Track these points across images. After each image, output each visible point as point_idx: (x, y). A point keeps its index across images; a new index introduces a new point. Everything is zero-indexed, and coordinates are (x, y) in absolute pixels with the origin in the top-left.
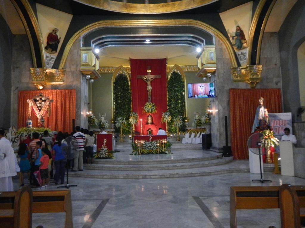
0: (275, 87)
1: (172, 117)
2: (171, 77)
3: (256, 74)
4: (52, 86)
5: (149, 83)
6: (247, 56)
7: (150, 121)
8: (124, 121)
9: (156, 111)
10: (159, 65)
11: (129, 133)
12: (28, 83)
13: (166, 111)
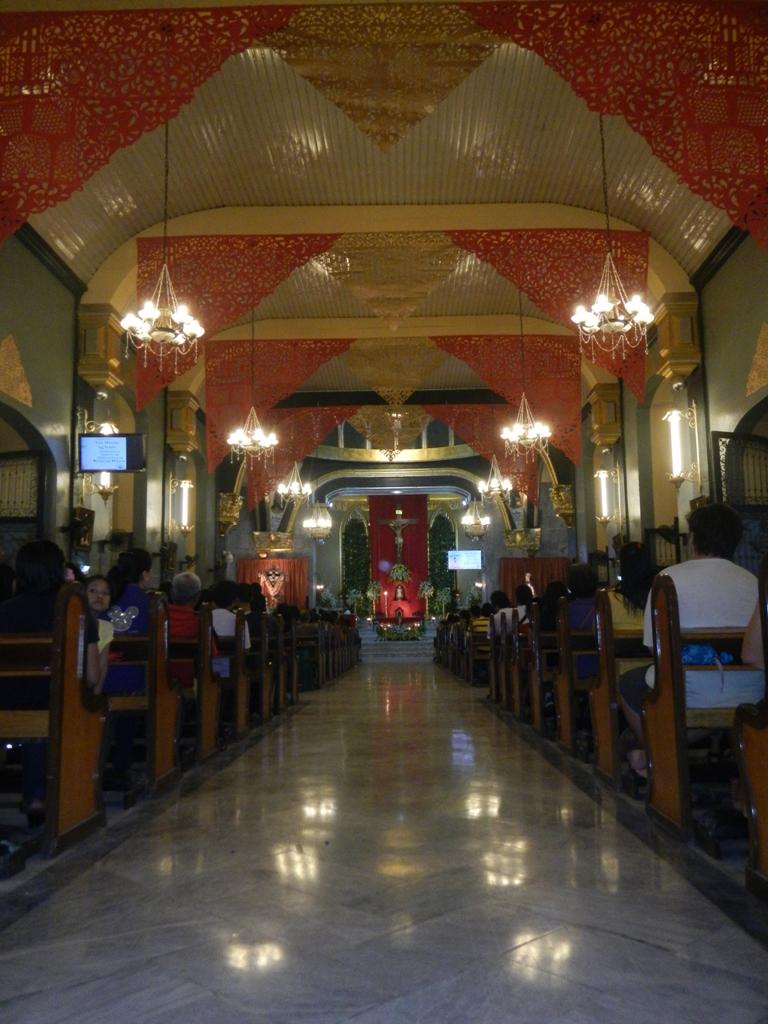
0: (561, 555)
1: (436, 589)
3: (533, 540)
4: (277, 553)
5: (399, 532)
6: (522, 518)
7: (400, 595)
8: (360, 595)
9: (410, 579)
10: (416, 505)
11: (368, 615)
12: (247, 549)
13: (424, 578)
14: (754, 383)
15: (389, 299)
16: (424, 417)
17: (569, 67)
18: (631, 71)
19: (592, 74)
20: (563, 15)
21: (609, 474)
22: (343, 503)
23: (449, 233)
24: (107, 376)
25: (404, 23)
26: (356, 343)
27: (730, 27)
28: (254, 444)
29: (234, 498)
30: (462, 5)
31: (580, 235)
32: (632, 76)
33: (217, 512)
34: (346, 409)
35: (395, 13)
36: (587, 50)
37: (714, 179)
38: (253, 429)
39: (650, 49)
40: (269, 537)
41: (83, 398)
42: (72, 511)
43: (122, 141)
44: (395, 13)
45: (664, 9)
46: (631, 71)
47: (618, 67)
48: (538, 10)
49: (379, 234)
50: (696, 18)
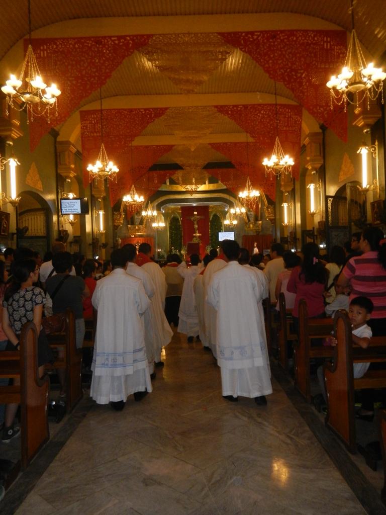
2: (213, 218)
5: (195, 222)
10: (203, 210)
14: (342, 177)
15: (190, 137)
16: (206, 175)
17: (262, 60)
18: (286, 62)
19: (271, 63)
20: (260, 38)
21: (288, 204)
22: (169, 209)
23: (216, 107)
24: (70, 173)
25: (196, 42)
26: (175, 147)
27: (327, 42)
28: (134, 201)
29: (120, 214)
30: (219, 34)
31: (272, 107)
32: (287, 65)
33: (113, 221)
34: (171, 171)
35: (192, 38)
36: (269, 53)
37: (318, 108)
38: (134, 194)
39: (295, 52)
40: (135, 228)
41: (60, 183)
42: (59, 232)
43: (84, 95)
44: (192, 38)
45: (301, 34)
46: (286, 62)
47: (281, 61)
48: (250, 36)
49: (185, 107)
50: (313, 39)
